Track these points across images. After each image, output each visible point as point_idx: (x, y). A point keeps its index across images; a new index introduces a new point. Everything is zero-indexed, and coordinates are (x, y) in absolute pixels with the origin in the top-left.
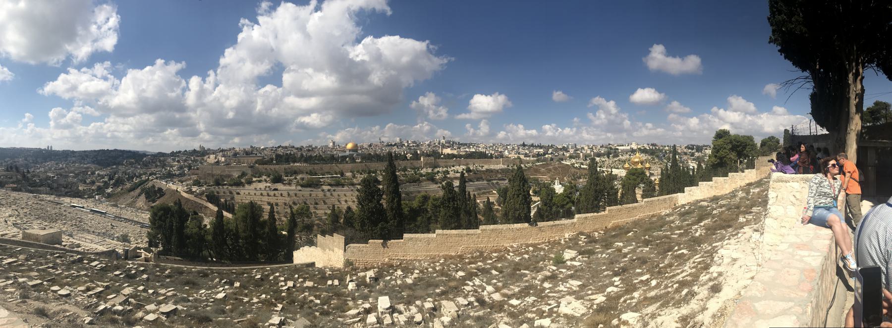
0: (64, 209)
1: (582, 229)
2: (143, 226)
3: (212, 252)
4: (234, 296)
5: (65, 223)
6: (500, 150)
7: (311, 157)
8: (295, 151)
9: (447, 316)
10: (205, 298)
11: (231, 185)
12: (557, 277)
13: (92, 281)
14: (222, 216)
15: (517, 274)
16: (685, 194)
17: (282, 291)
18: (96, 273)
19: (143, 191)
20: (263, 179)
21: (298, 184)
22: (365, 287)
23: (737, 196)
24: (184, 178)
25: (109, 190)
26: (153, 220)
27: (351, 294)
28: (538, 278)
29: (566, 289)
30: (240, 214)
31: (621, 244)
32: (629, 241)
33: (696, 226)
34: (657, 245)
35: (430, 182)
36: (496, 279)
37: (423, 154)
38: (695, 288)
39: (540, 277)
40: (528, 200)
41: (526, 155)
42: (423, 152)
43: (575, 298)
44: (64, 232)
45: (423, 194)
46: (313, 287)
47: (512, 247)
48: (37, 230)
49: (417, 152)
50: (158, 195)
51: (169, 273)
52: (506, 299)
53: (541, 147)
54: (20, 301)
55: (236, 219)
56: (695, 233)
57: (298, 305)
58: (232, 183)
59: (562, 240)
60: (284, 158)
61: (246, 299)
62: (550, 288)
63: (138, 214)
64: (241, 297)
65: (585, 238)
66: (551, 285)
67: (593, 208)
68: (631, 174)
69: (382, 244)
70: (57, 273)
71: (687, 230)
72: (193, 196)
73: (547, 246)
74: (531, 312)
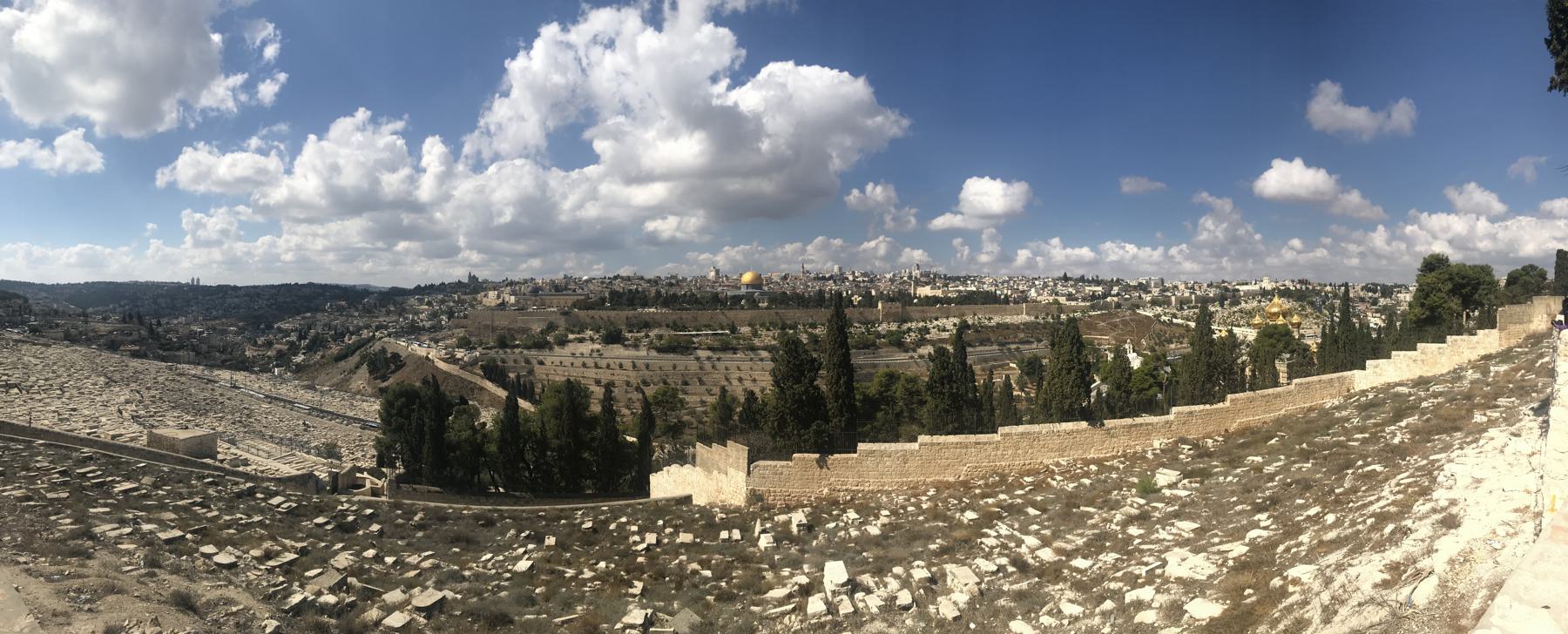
0: (220, 391)
1: (1183, 433)
2: (365, 425)
3: (496, 476)
4: (548, 566)
5: (222, 417)
6: (1021, 288)
7: (675, 295)
8: (645, 285)
9: (961, 592)
10: (493, 571)
11: (528, 348)
12: (1150, 517)
13: (273, 538)
14: (517, 406)
15: (1074, 514)
16: (1367, 371)
17: (636, 554)
18: (280, 521)
19: (363, 358)
20: (587, 337)
21: (651, 346)
22: (791, 543)
23: (1465, 377)
24: (440, 335)
25: (299, 358)
26: (387, 415)
27: (766, 556)
28: (1115, 521)
29: (1171, 537)
30: (550, 403)
31: (1259, 459)
32: (1272, 454)
33: (1393, 428)
34: (1325, 458)
35: (895, 349)
36: (1037, 523)
37: (881, 296)
38: (1408, 523)
39: (1118, 517)
40: (1087, 379)
41: (1070, 297)
42: (882, 293)
43: (1190, 551)
44: (220, 435)
45: (882, 371)
46: (694, 544)
47: (1058, 464)
48: (173, 429)
49: (870, 293)
50: (393, 367)
51: (421, 519)
52: (1064, 558)
53: (1097, 282)
54: (143, 571)
55: (542, 412)
56: (1392, 438)
57: (671, 581)
58: (530, 343)
59: (1150, 452)
60: (625, 298)
61: (570, 573)
62: (1140, 536)
63: (355, 403)
64: (561, 568)
65: (1190, 449)
66: (1142, 531)
67: (1202, 397)
68: (1266, 336)
69: (818, 461)
70: (209, 515)
71: (1377, 432)
72: (458, 368)
73: (1123, 463)
74: (1115, 579)
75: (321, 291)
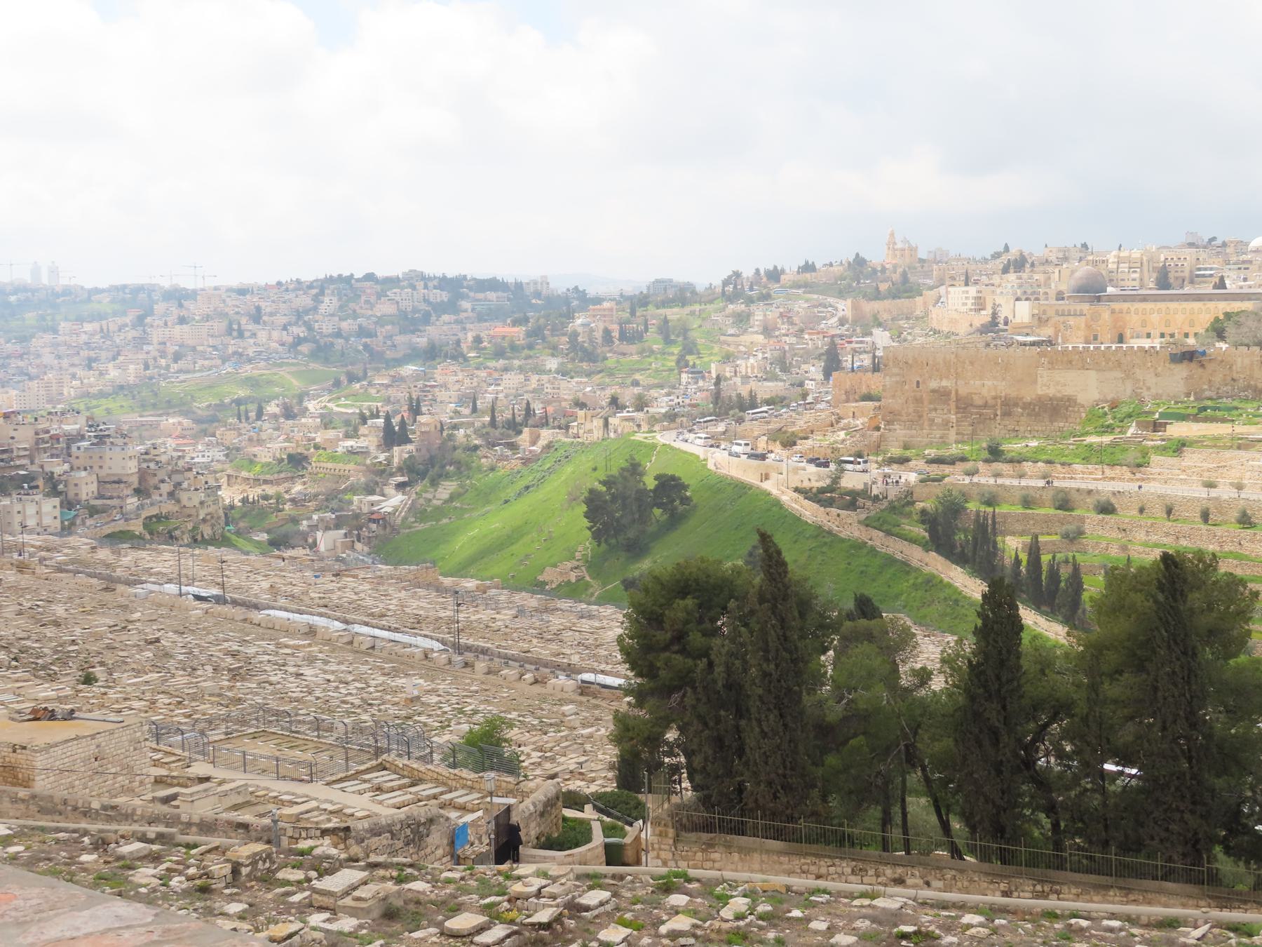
75: (443, 296)
